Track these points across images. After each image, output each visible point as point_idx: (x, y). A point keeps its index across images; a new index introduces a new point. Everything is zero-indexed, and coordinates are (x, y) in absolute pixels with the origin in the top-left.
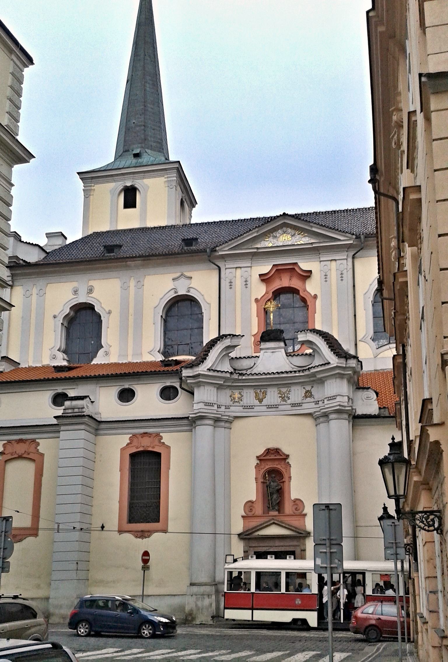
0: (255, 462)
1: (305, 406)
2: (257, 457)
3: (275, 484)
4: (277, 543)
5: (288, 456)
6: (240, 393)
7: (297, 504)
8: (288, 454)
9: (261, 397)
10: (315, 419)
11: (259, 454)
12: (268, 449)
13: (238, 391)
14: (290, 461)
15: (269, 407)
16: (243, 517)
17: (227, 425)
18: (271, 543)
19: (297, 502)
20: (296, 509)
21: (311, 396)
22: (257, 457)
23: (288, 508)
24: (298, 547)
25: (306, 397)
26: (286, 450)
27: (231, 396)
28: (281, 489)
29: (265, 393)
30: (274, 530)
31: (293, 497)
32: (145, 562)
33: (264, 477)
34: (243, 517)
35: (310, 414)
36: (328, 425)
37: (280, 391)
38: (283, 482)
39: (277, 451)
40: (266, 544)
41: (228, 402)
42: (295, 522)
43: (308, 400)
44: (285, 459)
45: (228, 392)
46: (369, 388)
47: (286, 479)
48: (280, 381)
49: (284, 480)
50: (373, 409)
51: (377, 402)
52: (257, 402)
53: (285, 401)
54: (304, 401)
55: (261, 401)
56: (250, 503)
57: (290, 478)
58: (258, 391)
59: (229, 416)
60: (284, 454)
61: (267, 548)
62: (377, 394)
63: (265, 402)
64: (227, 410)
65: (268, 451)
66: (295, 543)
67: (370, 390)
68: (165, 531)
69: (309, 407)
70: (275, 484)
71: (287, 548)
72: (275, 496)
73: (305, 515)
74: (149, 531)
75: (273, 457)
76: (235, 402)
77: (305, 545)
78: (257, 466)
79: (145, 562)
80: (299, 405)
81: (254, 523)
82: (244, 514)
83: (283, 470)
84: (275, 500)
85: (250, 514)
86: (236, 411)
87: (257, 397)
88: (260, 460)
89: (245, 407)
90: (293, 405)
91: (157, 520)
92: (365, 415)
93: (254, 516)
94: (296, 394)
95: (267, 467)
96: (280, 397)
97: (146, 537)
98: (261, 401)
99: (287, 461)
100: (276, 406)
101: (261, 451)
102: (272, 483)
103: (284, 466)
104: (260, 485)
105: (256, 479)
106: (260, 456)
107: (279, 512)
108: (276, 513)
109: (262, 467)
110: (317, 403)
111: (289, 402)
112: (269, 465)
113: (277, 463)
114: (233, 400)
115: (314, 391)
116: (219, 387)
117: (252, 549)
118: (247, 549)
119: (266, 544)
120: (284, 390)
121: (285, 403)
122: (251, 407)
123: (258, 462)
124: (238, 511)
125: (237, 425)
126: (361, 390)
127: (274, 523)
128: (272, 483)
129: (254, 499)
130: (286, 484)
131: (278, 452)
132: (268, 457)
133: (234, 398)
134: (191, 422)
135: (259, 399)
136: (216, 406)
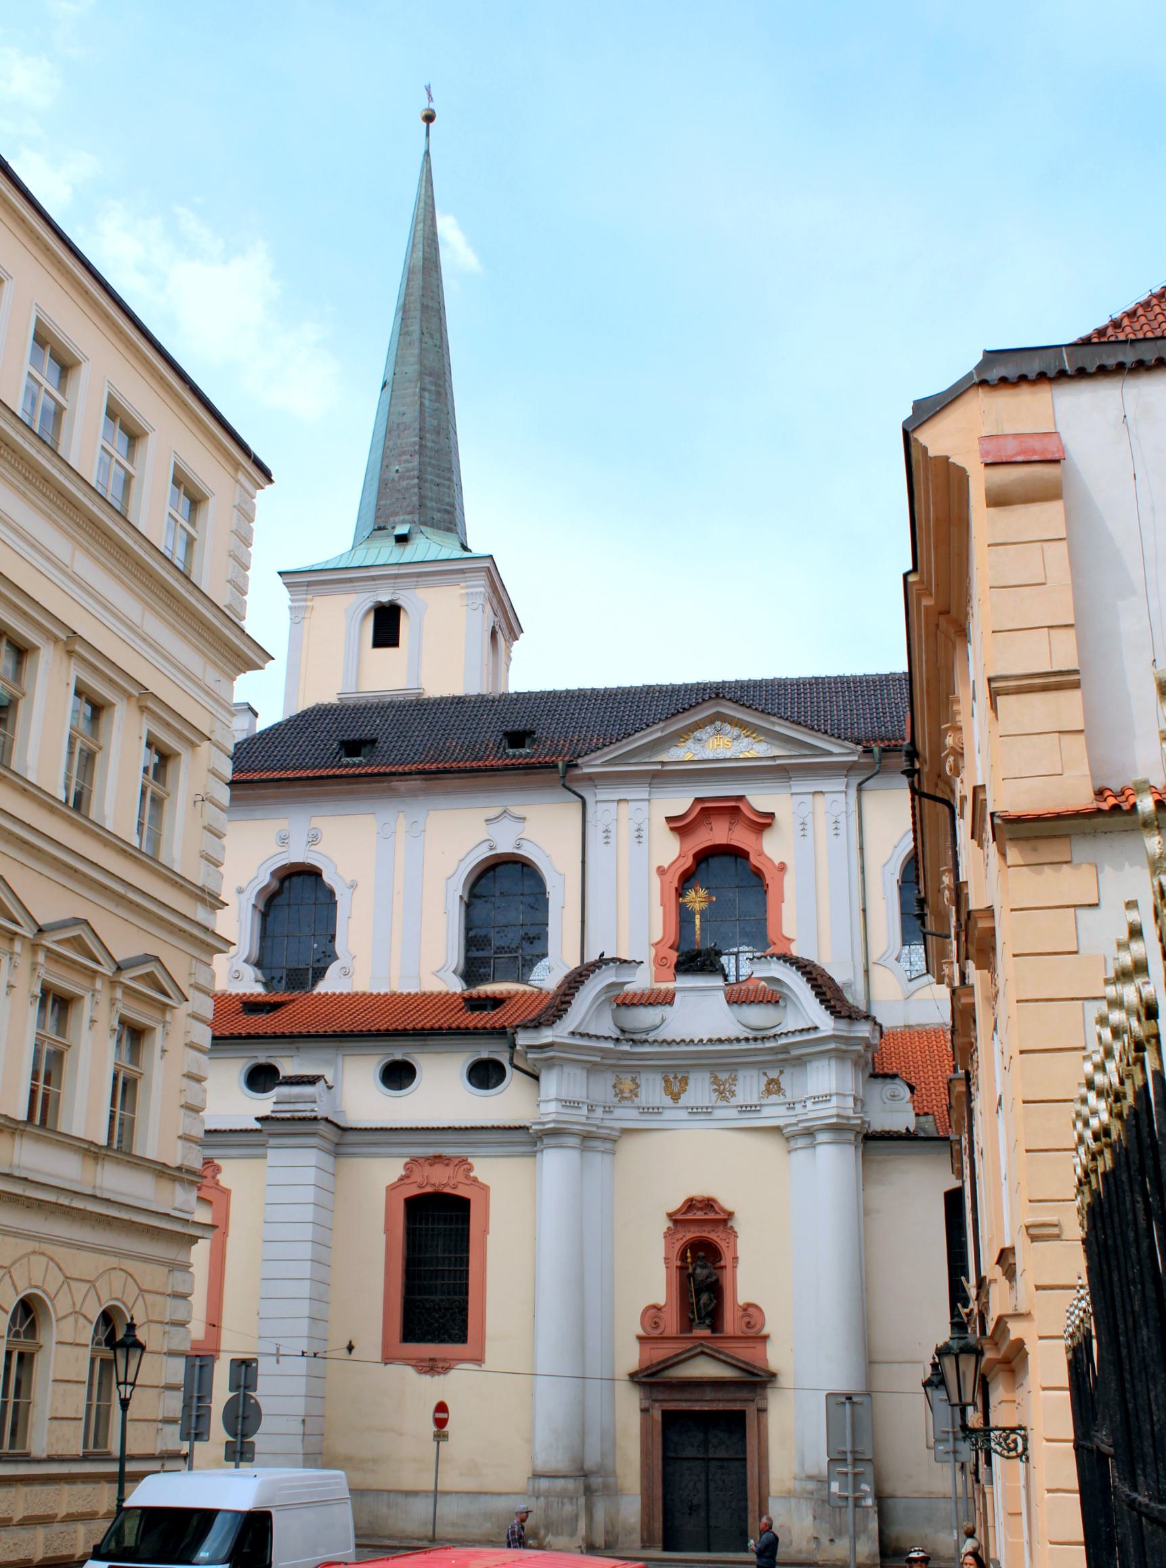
2: (670, 1215)
3: (705, 1272)
17: (608, 1145)
22: (670, 1215)
26: (726, 1201)
30: (704, 1369)
33: (683, 1257)
34: (640, 1338)
36: (814, 1153)
39: (709, 1204)
42: (743, 1352)
44: (725, 1221)
49: (722, 1263)
65: (691, 1204)
72: (704, 1298)
75: (700, 1215)
78: (669, 1235)
83: (723, 1245)
88: (676, 1222)
93: (662, 1339)
95: (689, 1236)
96: (715, 1090)
99: (730, 1224)
102: (698, 1271)
104: (675, 1274)
121: (724, 1103)
123: (670, 1224)
124: (631, 1326)
128: (698, 1271)
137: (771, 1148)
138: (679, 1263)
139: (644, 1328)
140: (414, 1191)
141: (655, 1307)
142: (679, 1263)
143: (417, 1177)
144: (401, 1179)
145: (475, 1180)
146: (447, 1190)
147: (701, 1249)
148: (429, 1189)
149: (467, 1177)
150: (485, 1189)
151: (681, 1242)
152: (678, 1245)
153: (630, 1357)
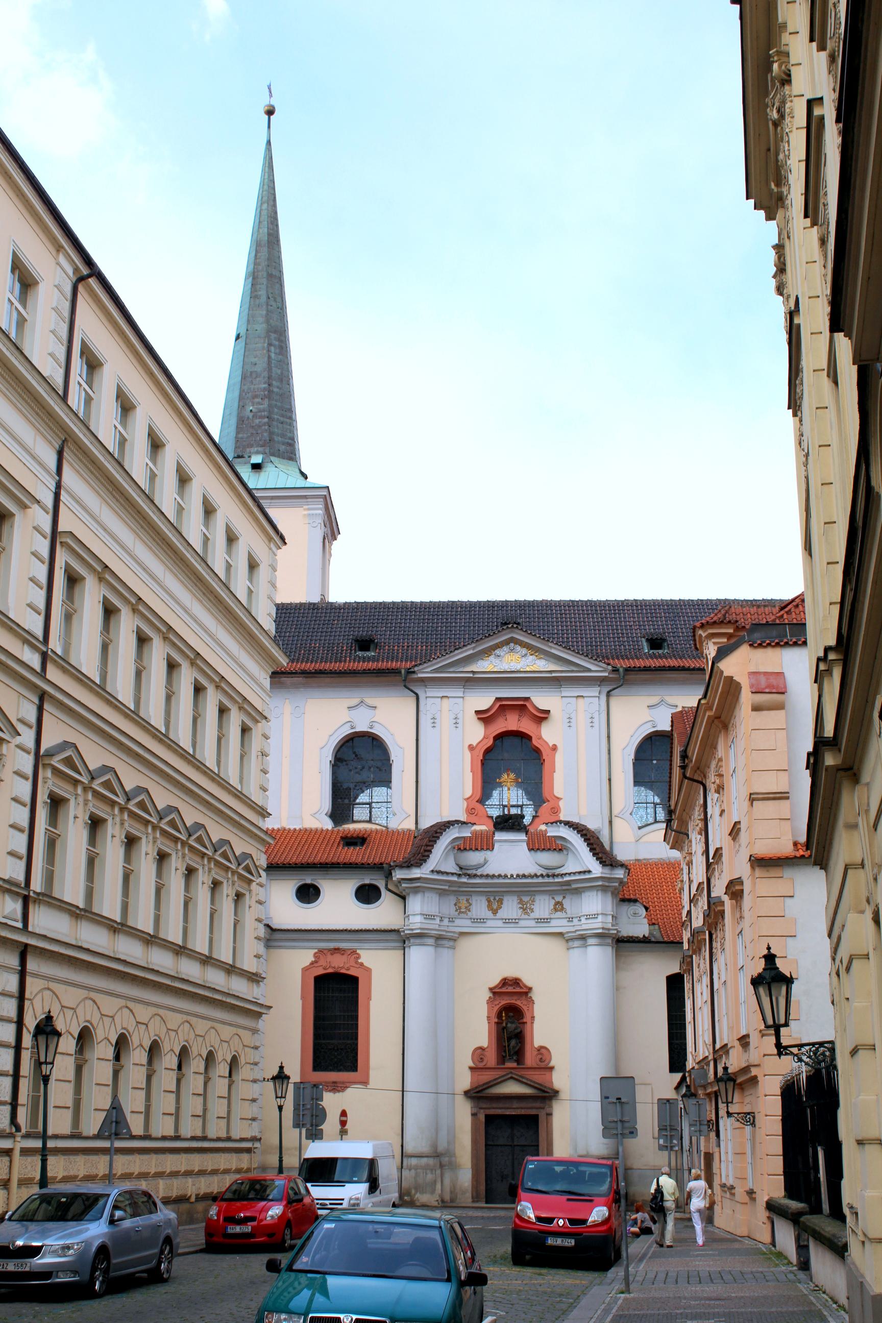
0: (488, 995)
1: (554, 923)
2: (491, 989)
3: (514, 1026)
5: (530, 989)
6: (467, 900)
7: (541, 1054)
9: (495, 907)
10: (567, 941)
11: (492, 985)
12: (505, 979)
13: (465, 898)
14: (535, 995)
15: (507, 921)
16: (471, 1068)
17: (451, 943)
19: (543, 1051)
20: (541, 1060)
21: (562, 909)
22: (491, 989)
23: (530, 1059)
25: (556, 910)
26: (527, 980)
27: (455, 905)
28: (521, 1032)
29: (500, 902)
30: (512, 1088)
31: (537, 1043)
32: (343, 1123)
33: (499, 1015)
34: (471, 1068)
35: (561, 934)
37: (521, 900)
38: (525, 1023)
39: (516, 982)
41: (452, 911)
42: (537, 1077)
43: (559, 914)
44: (526, 993)
45: (452, 899)
46: (635, 901)
47: (527, 1019)
48: (524, 889)
49: (524, 1020)
50: (641, 929)
51: (646, 920)
52: (489, 914)
53: (527, 913)
54: (552, 916)
55: (495, 912)
57: (533, 1018)
58: (492, 899)
59: (454, 932)
60: (526, 986)
62: (647, 909)
63: (502, 914)
64: (451, 924)
65: (505, 982)
66: (538, 1104)
67: (638, 904)
68: (365, 1082)
69: (559, 924)
70: (514, 1026)
72: (513, 1042)
73: (552, 1068)
74: (343, 1083)
75: (510, 989)
76: (460, 912)
77: (551, 1107)
78: (490, 1001)
79: (343, 1123)
80: (546, 921)
81: (486, 1077)
82: (472, 1065)
83: (525, 1008)
84: (514, 1047)
85: (481, 1065)
86: (462, 924)
87: (490, 907)
88: (494, 993)
89: (475, 921)
90: (539, 920)
91: (354, 1068)
92: (632, 937)
93: (485, 1068)
94: (542, 906)
95: (503, 1002)
97: (339, 1091)
98: (495, 912)
100: (515, 921)
101: (495, 981)
102: (509, 1025)
103: (525, 1002)
104: (494, 1026)
106: (495, 987)
107: (518, 1064)
108: (515, 1065)
110: (570, 920)
111: (532, 915)
113: (515, 998)
114: (458, 909)
115: (567, 903)
116: (442, 893)
118: (475, 1111)
120: (526, 899)
121: (526, 917)
122: (482, 921)
123: (491, 995)
124: (466, 1060)
125: (465, 944)
126: (626, 903)
127: (512, 1078)
128: (509, 1025)
129: (485, 1045)
130: (528, 1025)
132: (504, 990)
133: (460, 908)
134: (400, 939)
135: (492, 909)
136: (438, 919)
137: (556, 946)
138: (496, 1020)
139: (473, 1062)
140: (320, 972)
141: (481, 1048)
142: (496, 1020)
143: (322, 962)
144: (312, 963)
145: (362, 964)
146: (343, 971)
147: (511, 1010)
148: (330, 970)
149: (357, 962)
150: (368, 970)
151: (498, 1007)
152: (496, 1009)
153: (465, 1081)
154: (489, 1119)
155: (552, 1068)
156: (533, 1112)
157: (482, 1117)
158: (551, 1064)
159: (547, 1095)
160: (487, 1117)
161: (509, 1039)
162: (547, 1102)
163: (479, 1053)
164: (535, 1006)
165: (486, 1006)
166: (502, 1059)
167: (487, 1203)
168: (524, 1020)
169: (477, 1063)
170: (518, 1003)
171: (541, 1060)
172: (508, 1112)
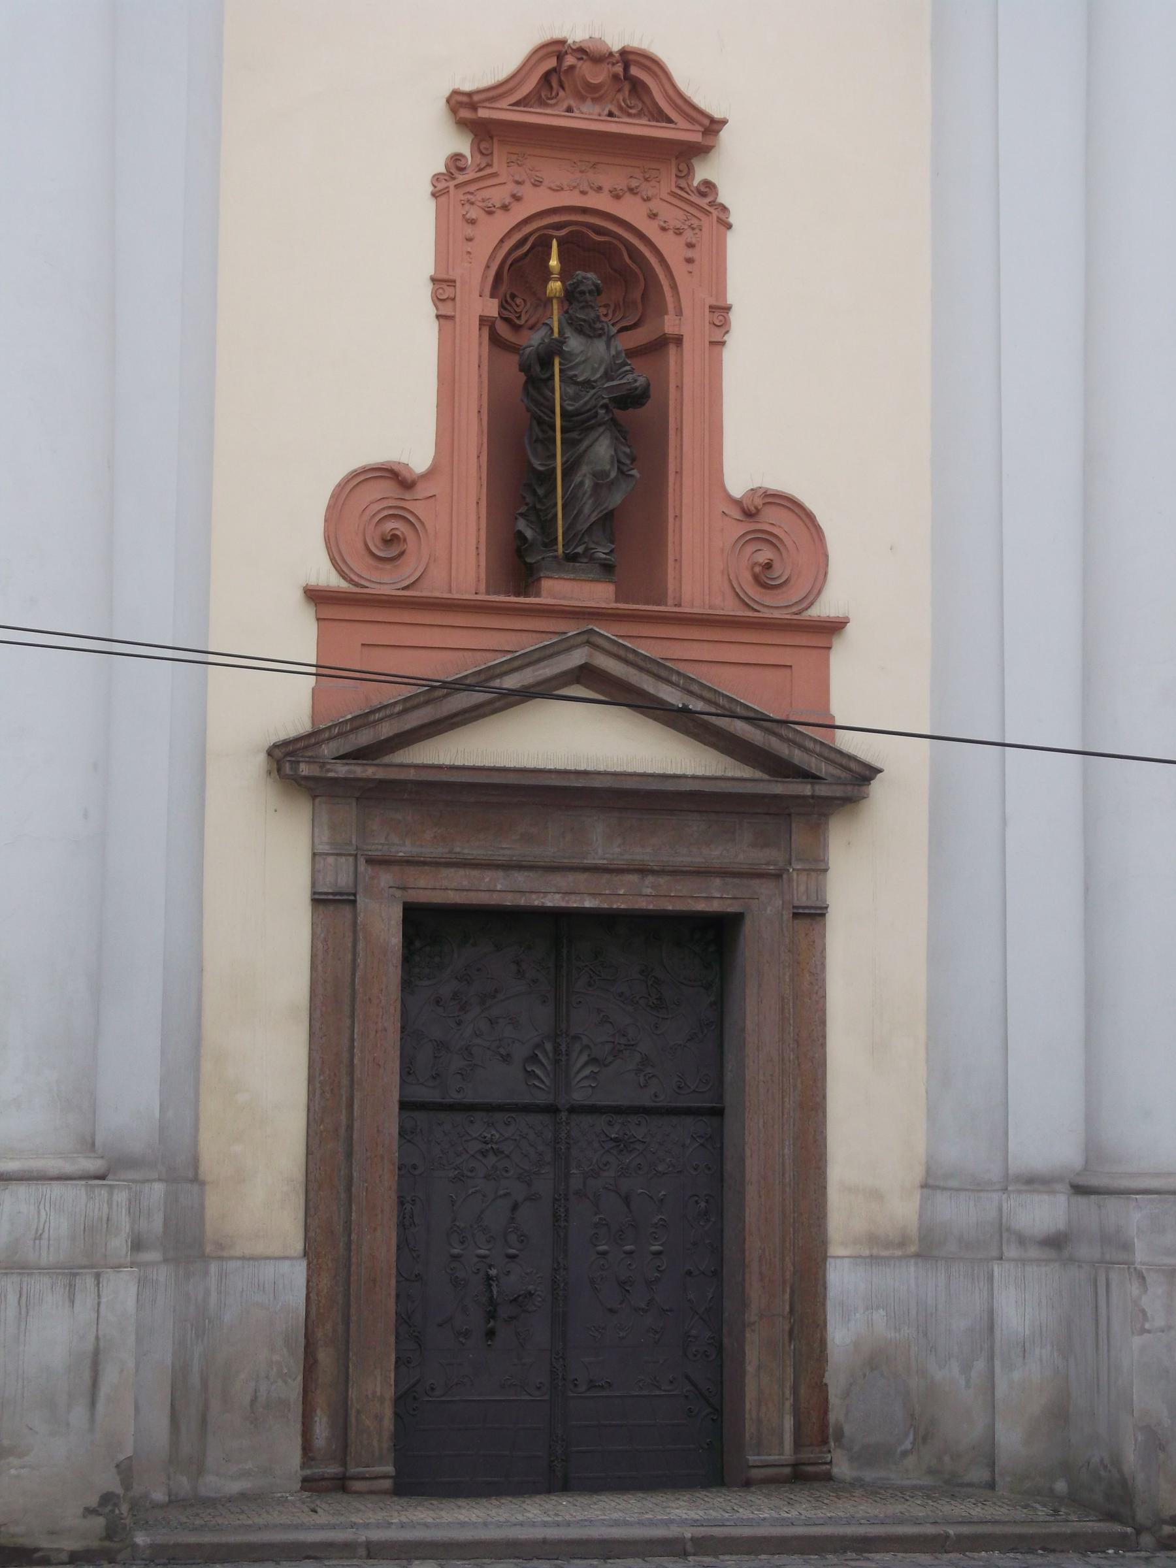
2: (465, 108)
4: (602, 841)
5: (713, 126)
7: (769, 539)
8: (717, 115)
12: (556, 49)
14: (730, 171)
16: (316, 596)
18: (553, 841)
19: (773, 518)
20: (764, 577)
22: (465, 108)
24: (764, 889)
31: (739, 479)
33: (517, 273)
34: (316, 596)
38: (662, 344)
39: (632, 76)
40: (509, 848)
42: (744, 678)
47: (685, 320)
56: (386, 488)
57: (721, 312)
61: (521, 879)
65: (560, 67)
66: (740, 851)
71: (683, 887)
72: (602, 449)
73: (834, 628)
75: (588, 117)
77: (819, 868)
78: (451, 182)
82: (327, 577)
84: (601, 483)
85: (385, 582)
95: (537, 201)
99: (702, 172)
102: (574, 343)
103: (672, 215)
104: (474, 343)
105: (443, 287)
108: (597, 594)
109: (498, 195)
112: (551, 189)
113: (613, 177)
117: (386, 878)
118: (341, 876)
119: (509, 848)
123: (463, 145)
127: (586, 674)
129: (418, 455)
130: (685, 366)
131: (637, 88)
141: (393, 475)
142: (492, 308)
151: (503, 223)
152: (493, 232)
154: (429, 929)
155: (834, 628)
156: (711, 898)
157: (385, 925)
158: (826, 607)
159: (798, 787)
160: (425, 926)
161: (579, 424)
162: (800, 838)
163: (376, 508)
164: (736, 245)
165: (428, 209)
166: (518, 565)
167: (411, 1483)
168: (670, 325)
169: (360, 565)
170: (630, 210)
171: (764, 577)
172: (552, 895)
